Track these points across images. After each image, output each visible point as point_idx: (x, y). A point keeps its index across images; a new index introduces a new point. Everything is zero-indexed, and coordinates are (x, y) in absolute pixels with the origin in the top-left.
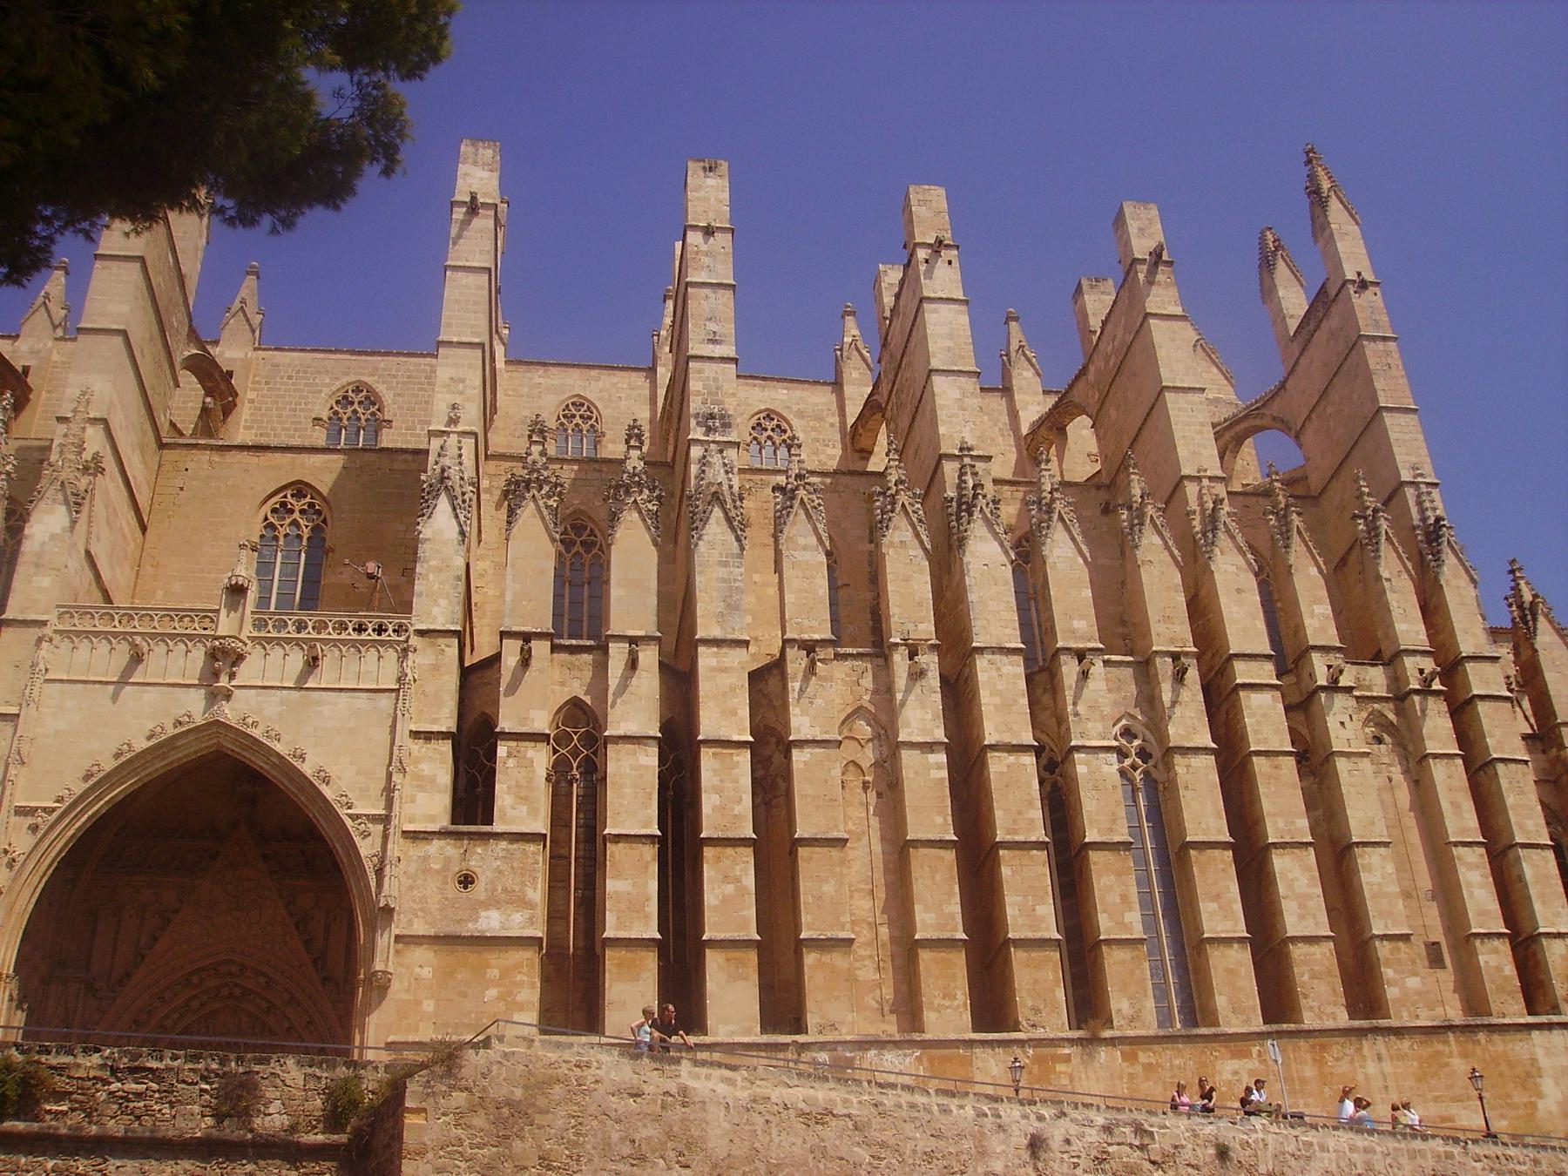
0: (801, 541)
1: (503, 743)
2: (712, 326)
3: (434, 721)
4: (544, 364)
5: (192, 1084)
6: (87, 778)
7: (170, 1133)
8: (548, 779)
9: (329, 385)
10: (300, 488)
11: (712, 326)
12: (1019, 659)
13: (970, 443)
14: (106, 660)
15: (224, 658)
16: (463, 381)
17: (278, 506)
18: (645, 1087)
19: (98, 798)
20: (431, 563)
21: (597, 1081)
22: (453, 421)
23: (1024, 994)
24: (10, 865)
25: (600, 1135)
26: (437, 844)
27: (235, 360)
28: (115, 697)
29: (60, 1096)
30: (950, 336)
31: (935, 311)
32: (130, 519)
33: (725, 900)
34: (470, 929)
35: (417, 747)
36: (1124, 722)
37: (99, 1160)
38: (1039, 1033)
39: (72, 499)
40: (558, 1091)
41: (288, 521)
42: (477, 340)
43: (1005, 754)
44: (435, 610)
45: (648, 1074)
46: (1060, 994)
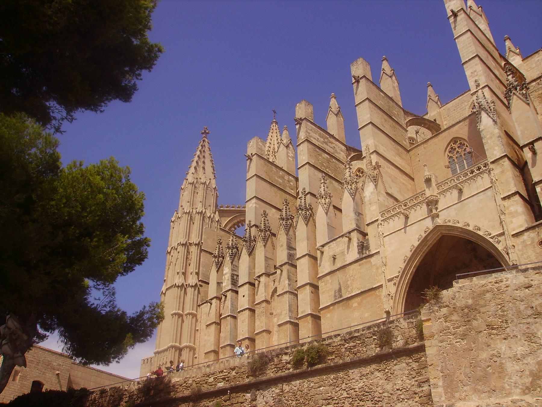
1: (538, 186)
3: (509, 191)
4: (537, 52)
5: (370, 338)
6: (405, 262)
7: (365, 357)
9: (466, 105)
10: (455, 140)
14: (399, 222)
15: (432, 203)
16: (475, 71)
17: (450, 150)
18: (532, 282)
19: (411, 267)
20: (487, 137)
21: (507, 287)
22: (478, 86)
24: (392, 299)
25: (514, 309)
26: (526, 234)
27: (435, 115)
28: (405, 232)
29: (332, 353)
35: (506, 203)
37: (346, 372)
39: (372, 179)
40: (488, 296)
41: (455, 153)
42: (475, 55)
44: (495, 152)
45: (533, 276)
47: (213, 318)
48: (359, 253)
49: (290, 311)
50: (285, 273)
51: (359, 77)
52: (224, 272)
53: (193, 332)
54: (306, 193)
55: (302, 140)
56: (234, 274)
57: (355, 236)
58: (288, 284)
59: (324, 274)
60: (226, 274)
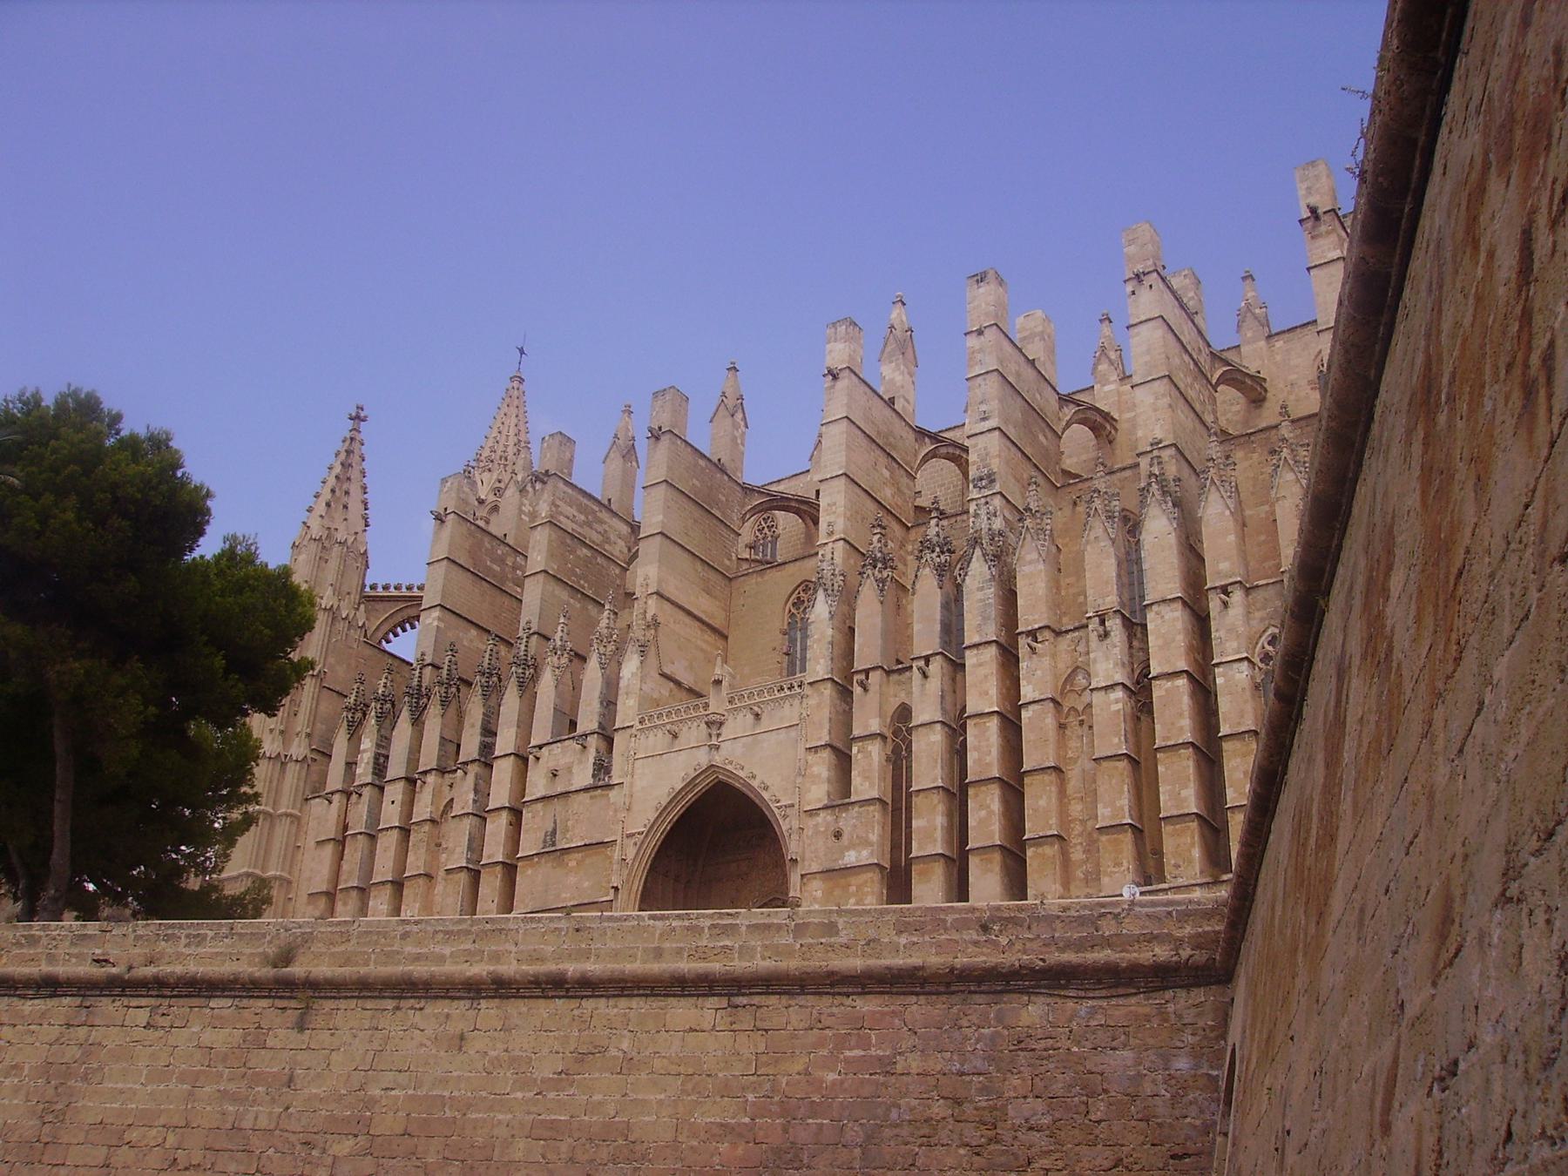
0: (1028, 557)
2: (983, 407)
3: (820, 739)
8: (888, 759)
11: (983, 407)
12: (1179, 605)
13: (1159, 436)
23: (1170, 856)
26: (822, 814)
30: (1148, 352)
31: (1138, 334)
32: (710, 639)
33: (981, 821)
34: (841, 863)
35: (811, 758)
36: (1269, 632)
38: (1180, 882)
42: (841, 472)
43: (1164, 682)
44: (818, 668)
46: (1196, 853)
47: (331, 831)
48: (594, 776)
49: (469, 848)
50: (471, 778)
51: (660, 428)
52: (362, 747)
53: (290, 849)
54: (531, 631)
55: (543, 518)
56: (379, 754)
57: (593, 741)
58: (474, 800)
59: (534, 797)
60: (365, 751)
